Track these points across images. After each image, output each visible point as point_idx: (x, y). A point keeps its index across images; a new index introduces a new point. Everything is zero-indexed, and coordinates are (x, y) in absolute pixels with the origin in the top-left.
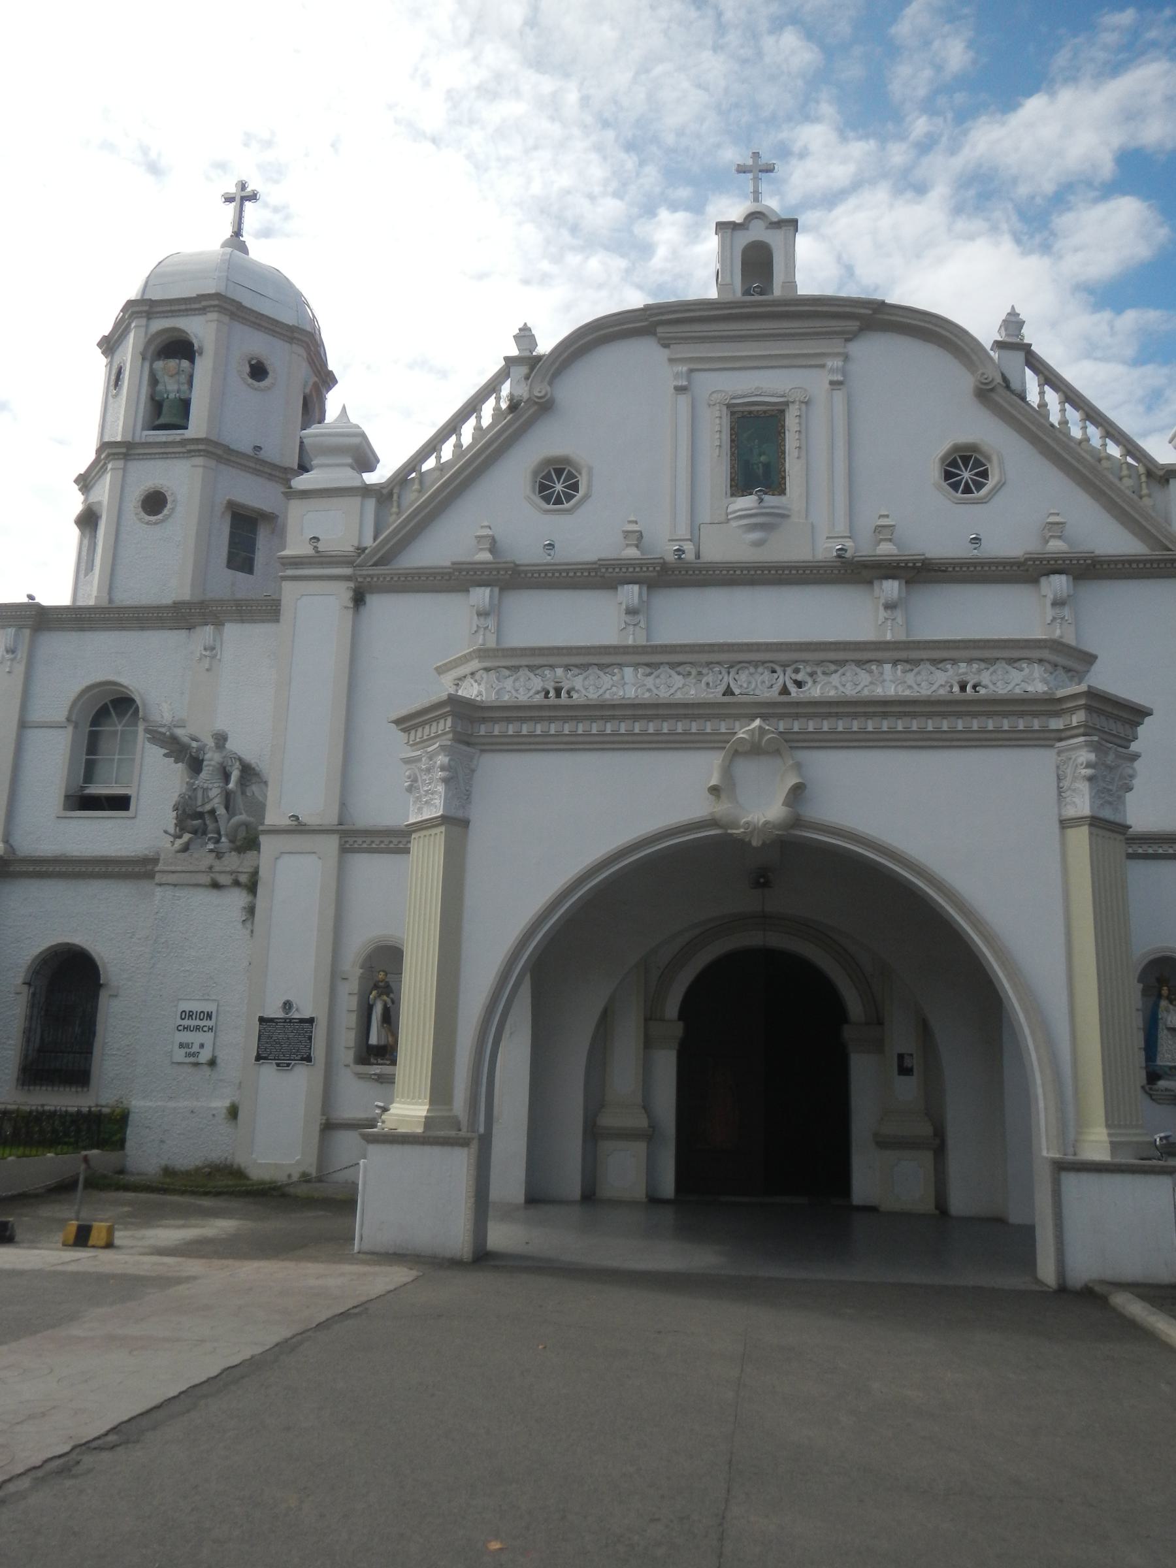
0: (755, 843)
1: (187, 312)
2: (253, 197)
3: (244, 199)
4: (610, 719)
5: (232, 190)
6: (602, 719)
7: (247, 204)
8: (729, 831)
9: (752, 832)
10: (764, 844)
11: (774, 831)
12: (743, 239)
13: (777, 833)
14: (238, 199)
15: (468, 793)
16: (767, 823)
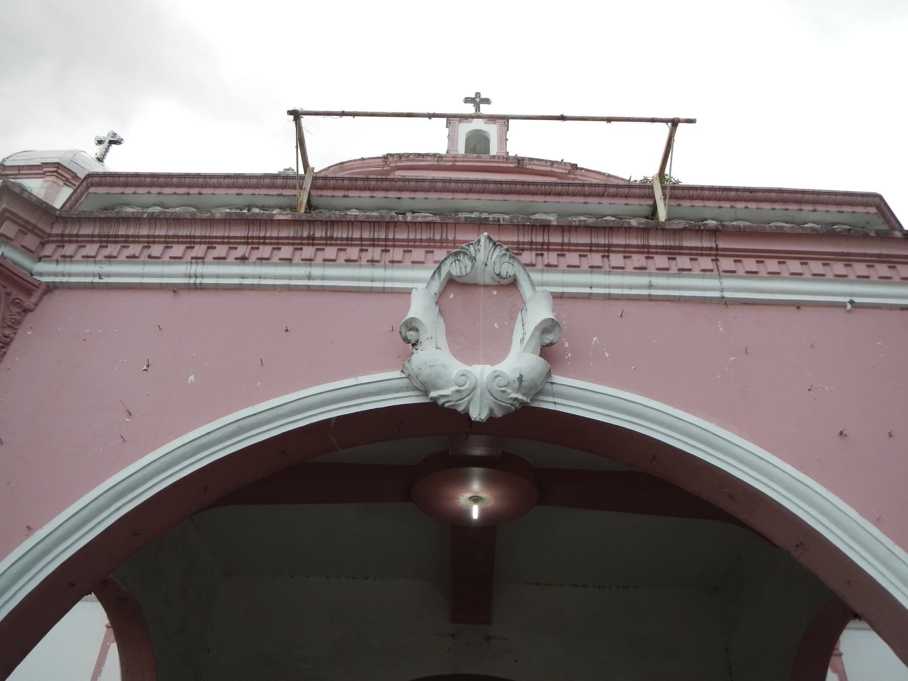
0: (478, 413)
1: (29, 176)
2: (117, 142)
3: (111, 142)
4: (259, 243)
5: (104, 134)
6: (247, 243)
7: (113, 145)
8: (433, 394)
9: (474, 389)
10: (491, 419)
11: (509, 391)
12: (465, 128)
13: (514, 395)
14: (106, 143)
15: (8, 340)
16: (498, 376)
